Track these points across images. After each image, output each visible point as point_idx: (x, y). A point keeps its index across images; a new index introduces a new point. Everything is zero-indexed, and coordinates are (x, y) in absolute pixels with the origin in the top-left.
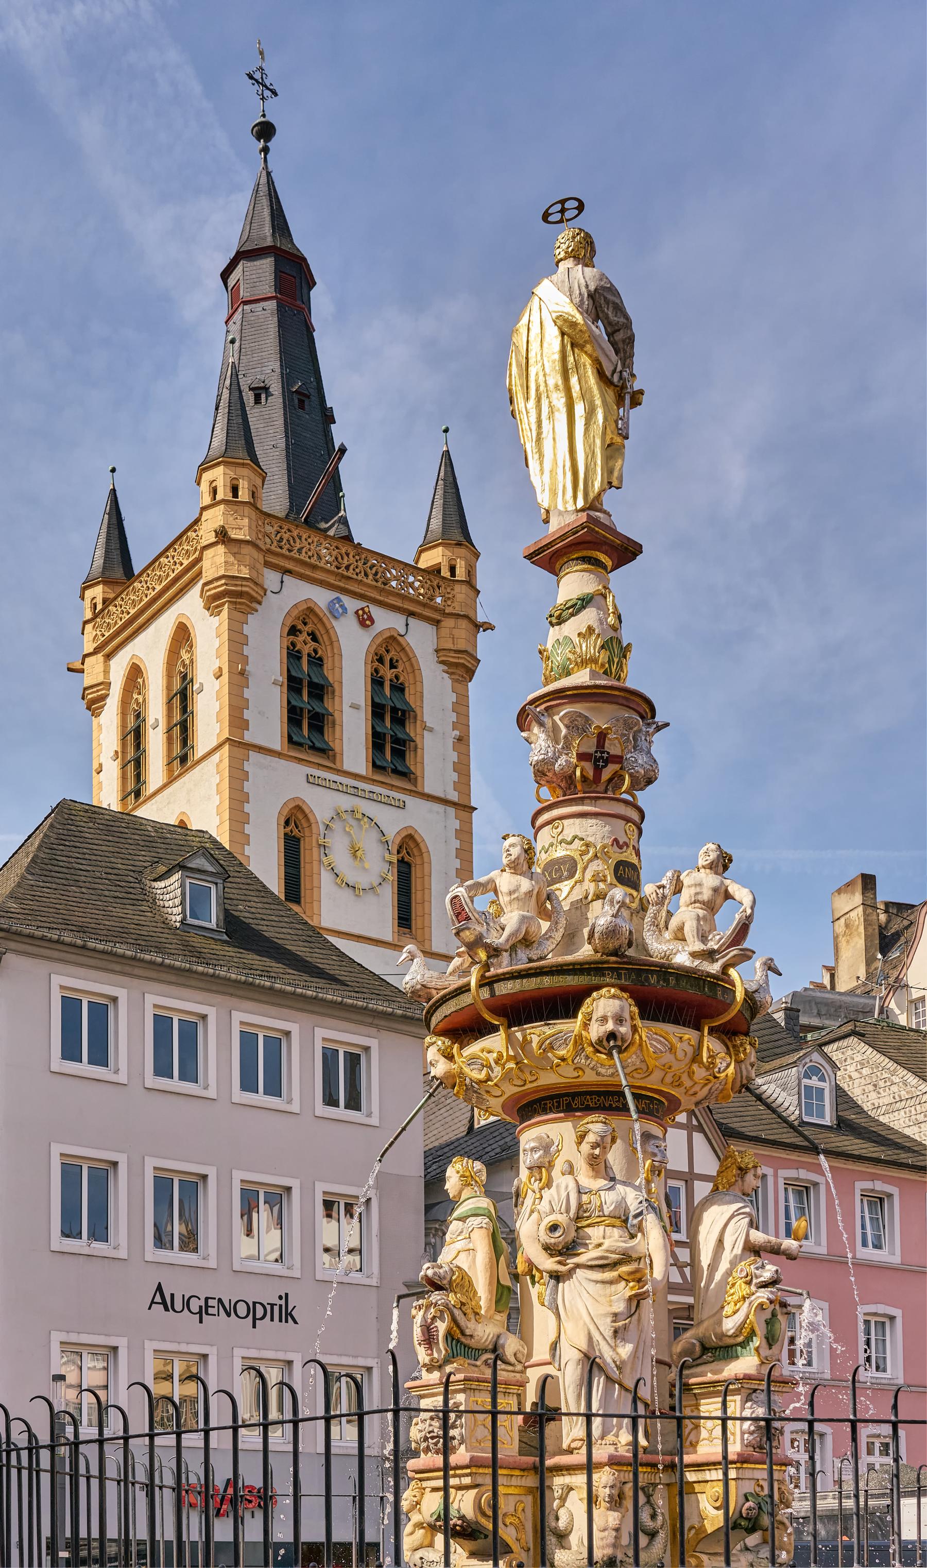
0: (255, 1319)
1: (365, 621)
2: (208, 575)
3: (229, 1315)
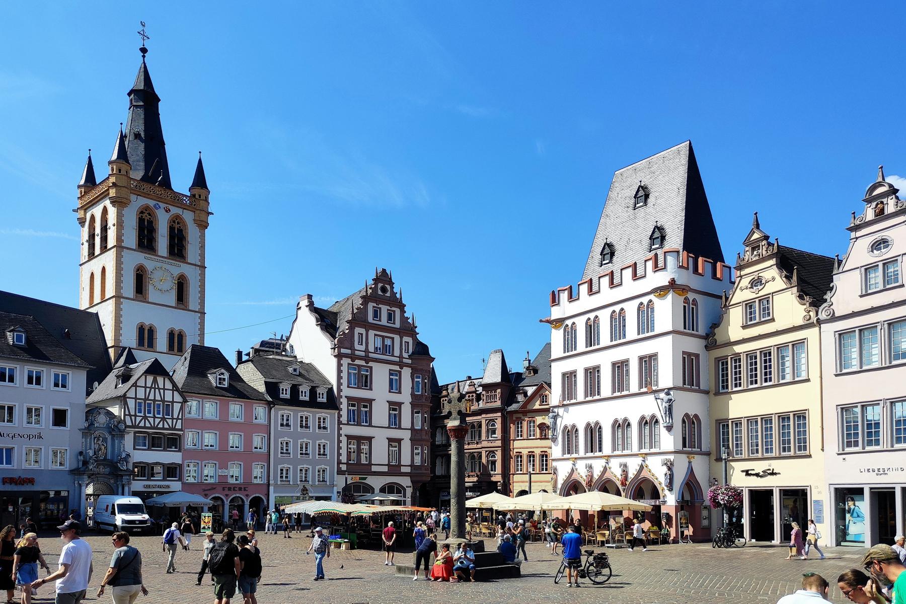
0: (30, 438)
1: (168, 211)
2: (111, 195)
3: (21, 437)
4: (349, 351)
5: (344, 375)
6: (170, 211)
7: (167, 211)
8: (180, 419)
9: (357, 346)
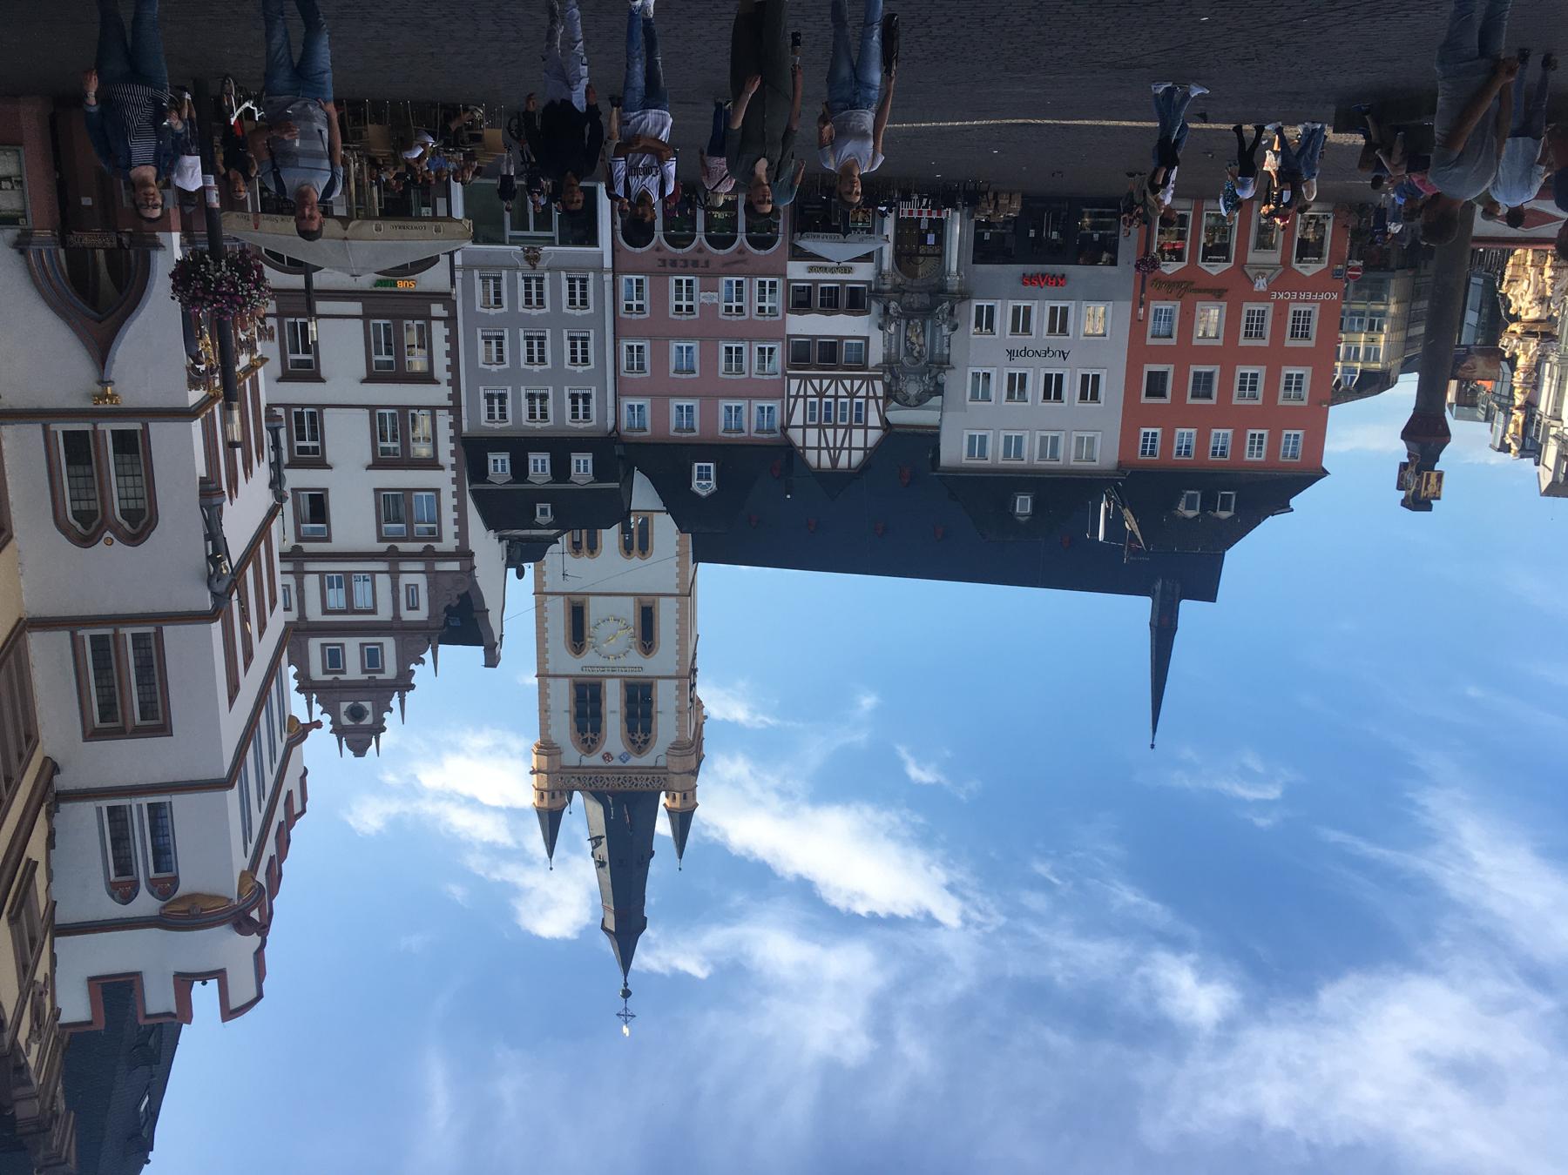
1: (607, 757)
4: (442, 566)
5: (448, 516)
6: (604, 758)
7: (608, 754)
8: (792, 397)
9: (421, 581)
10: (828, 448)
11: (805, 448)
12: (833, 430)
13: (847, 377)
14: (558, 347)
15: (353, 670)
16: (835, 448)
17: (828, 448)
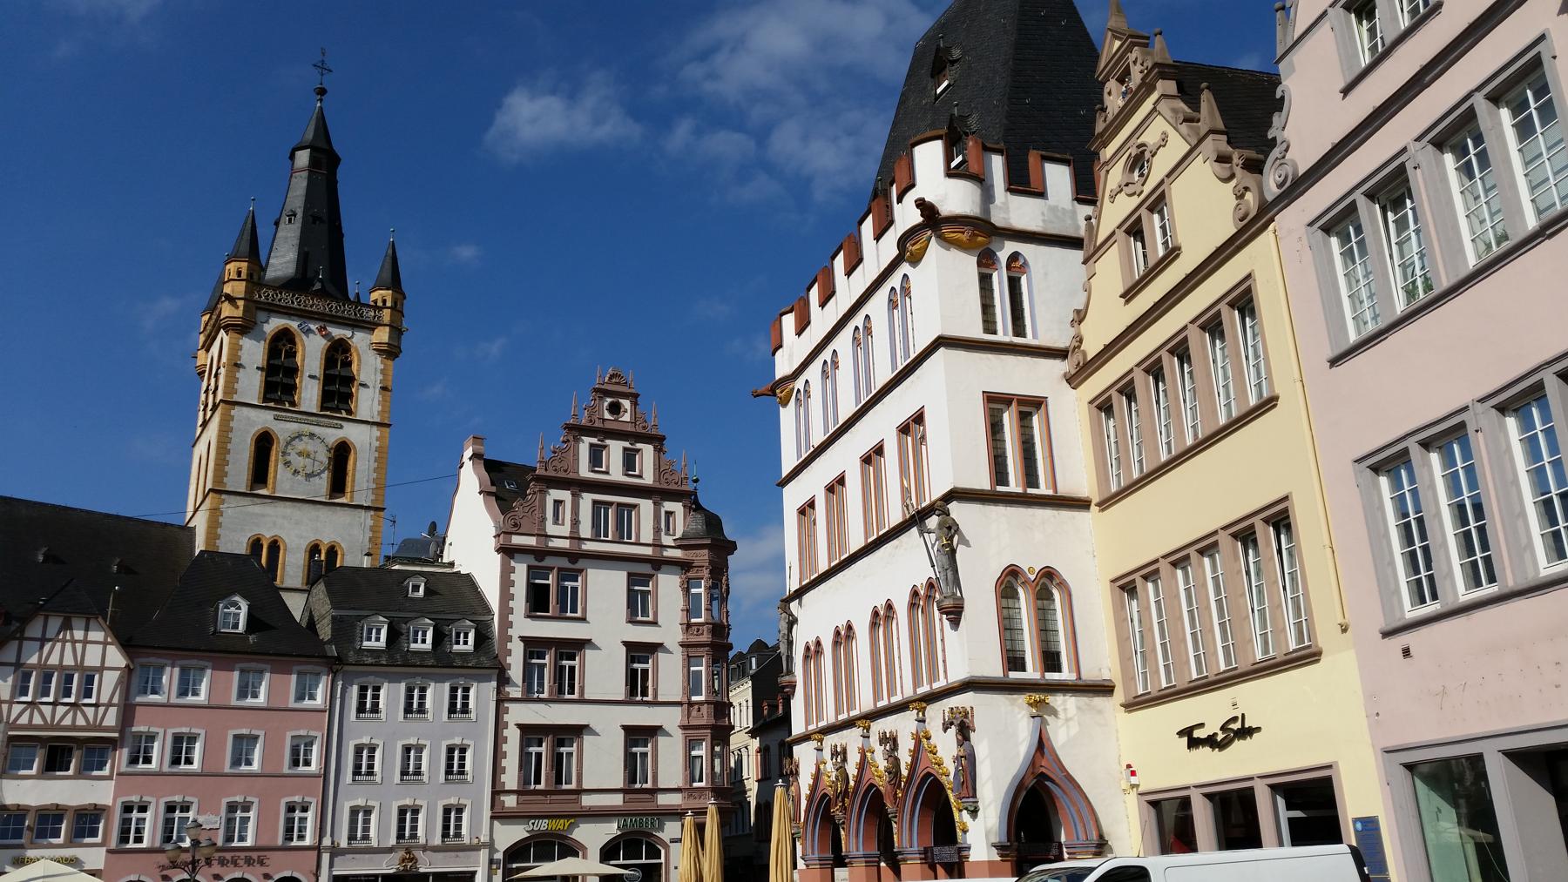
9: (551, 529)
10: (74, 642)
11: (105, 644)
12: (64, 664)
13: (37, 728)
14: (432, 762)
15: (616, 448)
16: (64, 641)
17: (74, 642)
